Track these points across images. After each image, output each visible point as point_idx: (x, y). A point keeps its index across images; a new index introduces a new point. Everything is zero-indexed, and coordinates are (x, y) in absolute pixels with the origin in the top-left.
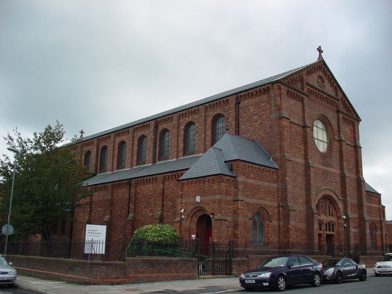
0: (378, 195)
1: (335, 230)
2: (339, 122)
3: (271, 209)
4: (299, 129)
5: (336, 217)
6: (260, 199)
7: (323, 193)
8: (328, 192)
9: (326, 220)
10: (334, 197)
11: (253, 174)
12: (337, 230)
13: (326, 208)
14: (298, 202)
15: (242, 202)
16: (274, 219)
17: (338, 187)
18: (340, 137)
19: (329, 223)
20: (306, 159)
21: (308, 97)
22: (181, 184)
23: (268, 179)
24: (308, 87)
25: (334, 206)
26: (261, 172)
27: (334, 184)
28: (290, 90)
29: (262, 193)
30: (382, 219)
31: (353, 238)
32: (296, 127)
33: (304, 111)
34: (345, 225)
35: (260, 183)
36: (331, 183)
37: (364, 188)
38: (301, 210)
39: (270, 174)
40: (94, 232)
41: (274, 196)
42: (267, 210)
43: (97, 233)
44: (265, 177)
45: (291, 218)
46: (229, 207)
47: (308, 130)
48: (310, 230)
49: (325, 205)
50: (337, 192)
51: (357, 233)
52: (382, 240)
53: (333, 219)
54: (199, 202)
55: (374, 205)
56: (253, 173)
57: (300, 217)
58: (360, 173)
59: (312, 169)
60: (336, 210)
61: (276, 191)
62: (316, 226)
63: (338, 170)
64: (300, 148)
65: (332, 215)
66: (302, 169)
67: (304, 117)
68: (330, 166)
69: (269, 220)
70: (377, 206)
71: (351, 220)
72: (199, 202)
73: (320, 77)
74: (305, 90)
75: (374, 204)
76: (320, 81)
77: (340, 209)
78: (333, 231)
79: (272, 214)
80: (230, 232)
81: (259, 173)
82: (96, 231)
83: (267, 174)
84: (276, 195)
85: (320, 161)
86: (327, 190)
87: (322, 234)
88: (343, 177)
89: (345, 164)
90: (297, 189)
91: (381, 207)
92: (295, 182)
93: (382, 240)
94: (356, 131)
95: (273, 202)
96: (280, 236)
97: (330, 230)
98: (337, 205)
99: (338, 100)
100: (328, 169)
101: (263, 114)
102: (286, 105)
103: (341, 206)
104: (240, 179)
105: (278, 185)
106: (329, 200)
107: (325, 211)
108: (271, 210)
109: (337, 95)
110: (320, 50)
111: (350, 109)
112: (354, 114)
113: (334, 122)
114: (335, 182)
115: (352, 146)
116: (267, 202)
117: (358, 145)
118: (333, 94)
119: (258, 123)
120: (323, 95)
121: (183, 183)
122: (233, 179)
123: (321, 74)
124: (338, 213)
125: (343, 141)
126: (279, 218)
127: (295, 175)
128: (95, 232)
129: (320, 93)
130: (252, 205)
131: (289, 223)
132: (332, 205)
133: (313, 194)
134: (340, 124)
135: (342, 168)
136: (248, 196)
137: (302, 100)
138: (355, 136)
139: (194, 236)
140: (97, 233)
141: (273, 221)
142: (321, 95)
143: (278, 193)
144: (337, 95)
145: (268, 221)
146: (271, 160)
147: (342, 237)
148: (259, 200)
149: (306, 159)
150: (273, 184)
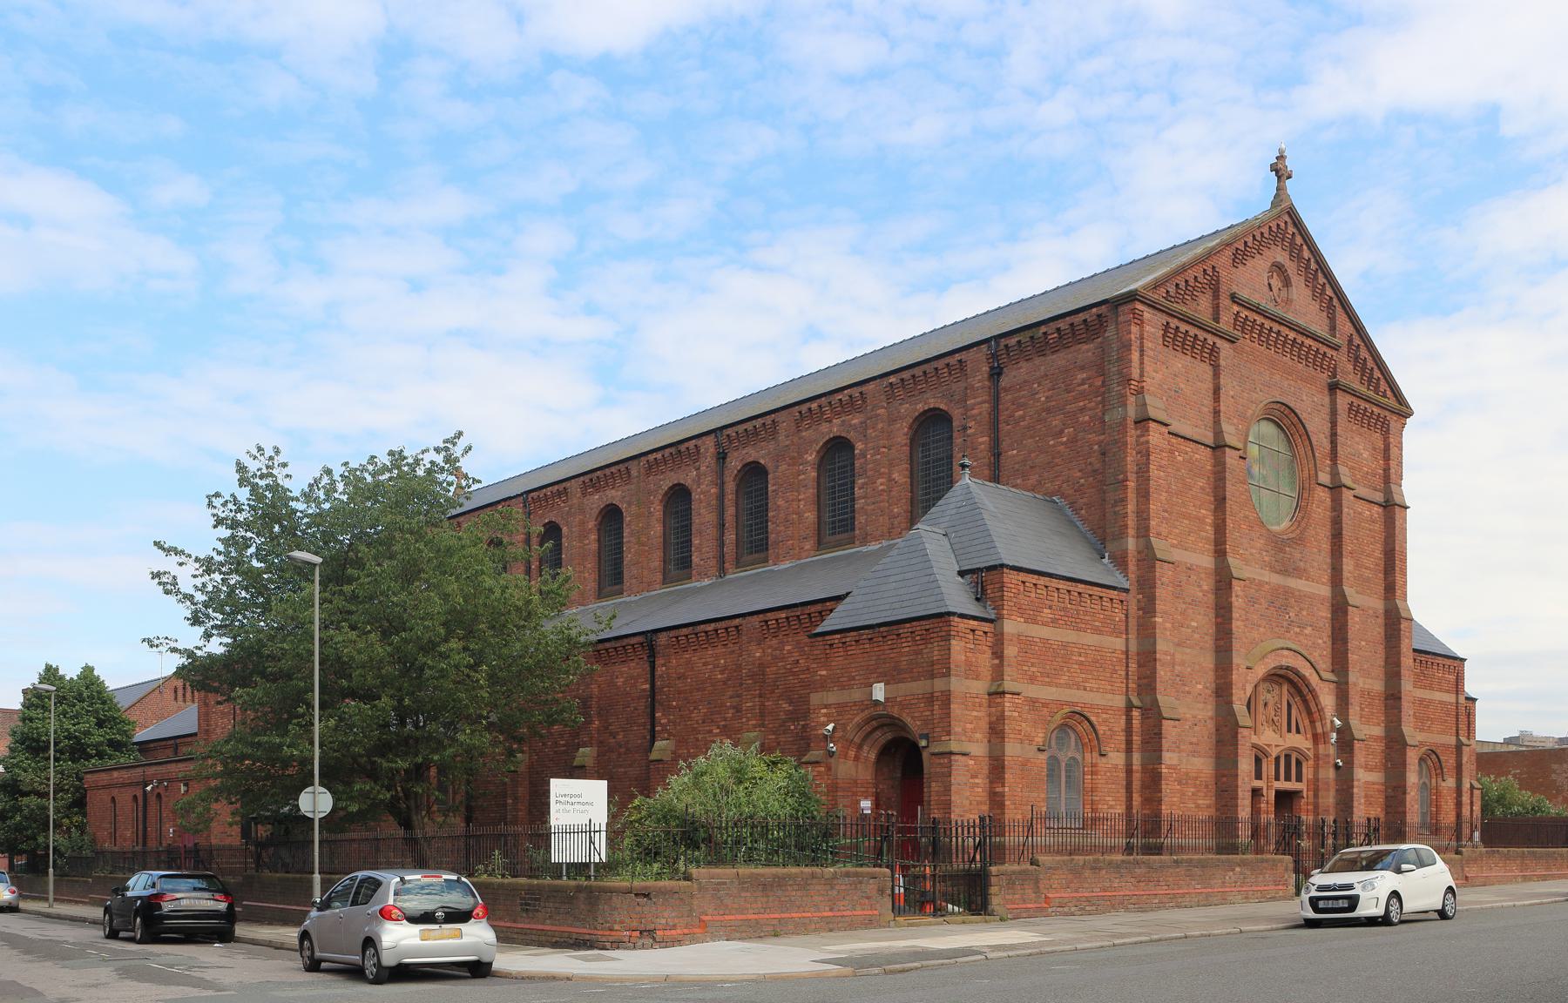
0: (1456, 663)
1: (1304, 779)
2: (1334, 424)
3: (1104, 716)
4: (1203, 456)
5: (1309, 736)
6: (1068, 686)
7: (1271, 663)
8: (1287, 657)
9: (1276, 746)
11: (1049, 611)
12: (1311, 777)
13: (1277, 710)
14: (1189, 693)
15: (1014, 696)
16: (1113, 746)
17: (1320, 641)
18: (1335, 474)
19: (1288, 757)
20: (1220, 552)
21: (1233, 342)
22: (822, 647)
23: (1097, 624)
24: (1236, 308)
25: (1305, 702)
26: (1074, 602)
27: (1308, 631)
28: (1174, 323)
29: (1077, 667)
30: (1463, 739)
31: (1363, 801)
33: (1216, 391)
34: (1339, 761)
35: (1070, 636)
37: (1407, 641)
38: (1200, 717)
39: (1102, 605)
40: (573, 800)
41: (1115, 675)
42: (1093, 719)
43: (583, 804)
44: (1087, 618)
45: (1165, 744)
46: (975, 713)
47: (1231, 457)
48: (1224, 779)
49: (1276, 698)
50: (1315, 656)
51: (1376, 786)
52: (1459, 804)
53: (1301, 742)
54: (883, 700)
55: (1438, 696)
56: (1050, 608)
57: (1194, 740)
58: (1398, 593)
59: (1237, 587)
60: (1310, 713)
61: (1120, 660)
62: (1245, 765)
63: (1323, 584)
64: (1201, 520)
65: (1298, 731)
66: (1205, 588)
67: (1217, 413)
68: (1298, 573)
69: (1097, 749)
70: (1450, 698)
71: (1357, 745)
72: (883, 700)
73: (1278, 268)
74: (1226, 323)
75: (1440, 690)
76: (1276, 283)
77: (1326, 710)
78: (1299, 779)
79: (1108, 733)
80: (980, 790)
81: (1069, 606)
82: (580, 796)
83: (1092, 606)
84: (1119, 672)
85: (1266, 559)
86: (1286, 652)
87: (1262, 789)
88: (1340, 608)
89: (1348, 565)
90: (1188, 651)
91: (1462, 699)
92: (1183, 629)
93: (1459, 804)
94: (1394, 451)
95: (1110, 696)
96: (1129, 799)
97: (1288, 778)
98: (1315, 697)
99: (1336, 348)
101: (1082, 410)
102: (1158, 376)
103: (1327, 700)
104: (1011, 626)
105: (1127, 639)
106: (1291, 682)
107: (1275, 719)
108: (1105, 721)
109: (1333, 329)
110: (1280, 171)
111: (1377, 374)
112: (1389, 393)
113: (1317, 425)
114: (1311, 626)
115: (1377, 504)
116: (1092, 694)
117: (1397, 499)
118: (1319, 326)
119: (1065, 439)
120: (1285, 331)
121: (829, 642)
122: (987, 627)
123: (1281, 256)
124: (1318, 724)
125: (1345, 486)
126: (1129, 742)
127: (1184, 606)
128: (578, 800)
129: (1276, 327)
130: (1045, 705)
131: (1159, 760)
132: (1298, 699)
133: (1238, 665)
134: (1339, 431)
135: (1336, 580)
136: (1032, 679)
137: (1214, 350)
138: (1387, 470)
139: (866, 805)
140: (583, 804)
141: (1110, 754)
142: (1278, 333)
143: (1127, 666)
144: (1333, 329)
145: (1095, 754)
146: (1106, 561)
147: (1329, 799)
148: (1068, 691)
149: (1220, 552)
150: (1113, 639)
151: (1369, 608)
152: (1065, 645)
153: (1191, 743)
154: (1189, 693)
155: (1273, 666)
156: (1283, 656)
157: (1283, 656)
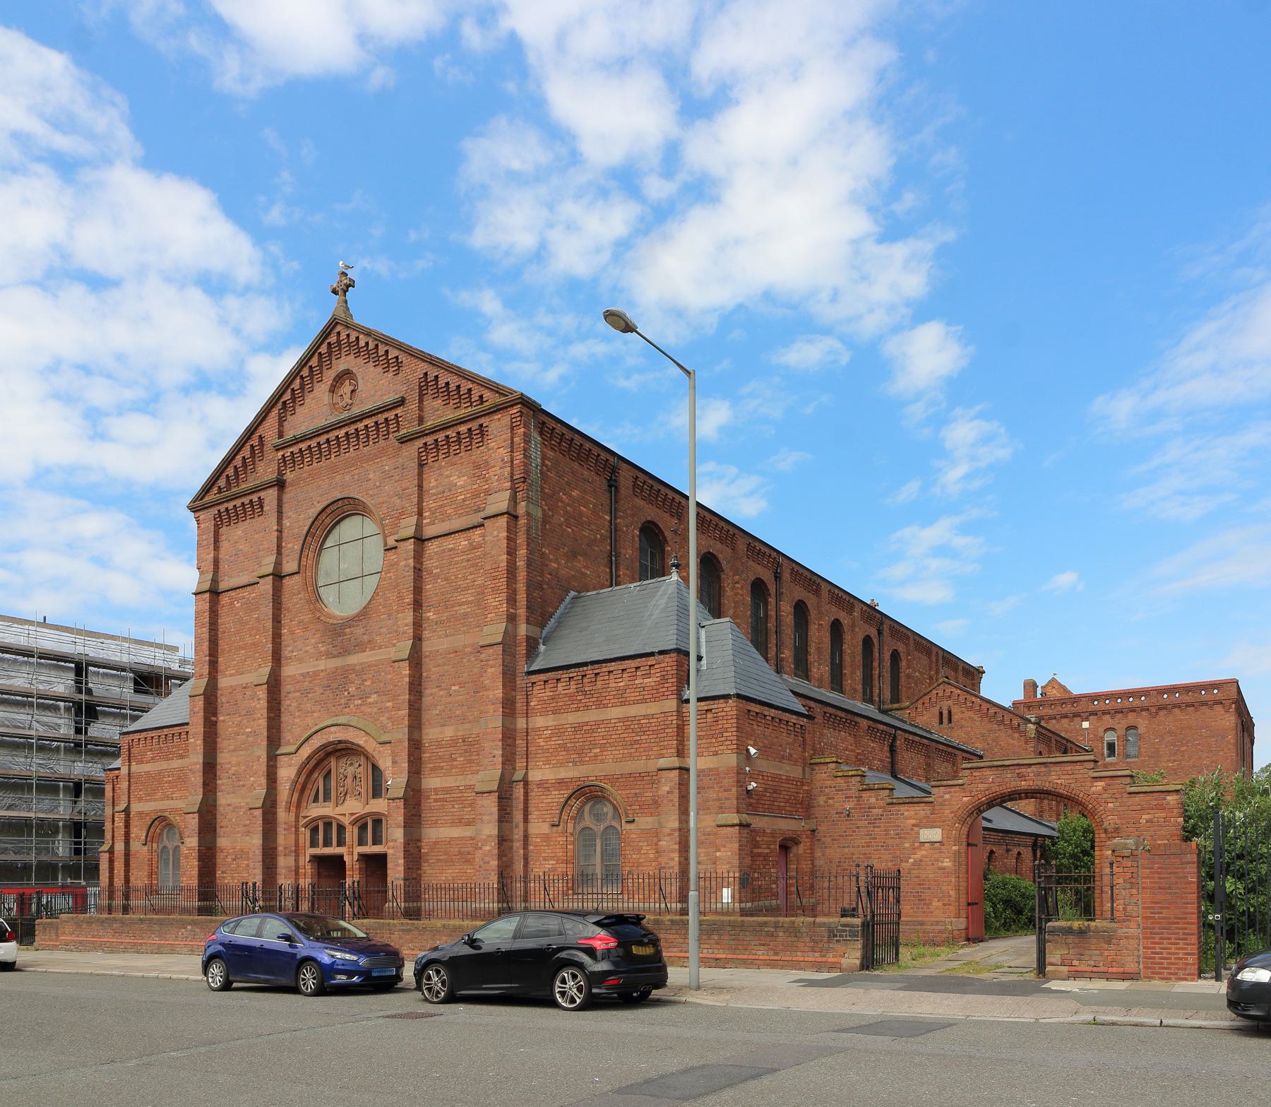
6: (162, 799)
9: (352, 814)
10: (361, 743)
14: (244, 786)
27: (374, 698)
32: (245, 593)
35: (163, 765)
56: (151, 750)
85: (322, 649)
90: (242, 753)
100: (352, 660)
116: (176, 801)
127: (239, 719)
151: (465, 646)
152: (160, 772)
153: (245, 826)
154: (244, 786)
155: (319, 744)
156: (331, 733)
157: (331, 733)
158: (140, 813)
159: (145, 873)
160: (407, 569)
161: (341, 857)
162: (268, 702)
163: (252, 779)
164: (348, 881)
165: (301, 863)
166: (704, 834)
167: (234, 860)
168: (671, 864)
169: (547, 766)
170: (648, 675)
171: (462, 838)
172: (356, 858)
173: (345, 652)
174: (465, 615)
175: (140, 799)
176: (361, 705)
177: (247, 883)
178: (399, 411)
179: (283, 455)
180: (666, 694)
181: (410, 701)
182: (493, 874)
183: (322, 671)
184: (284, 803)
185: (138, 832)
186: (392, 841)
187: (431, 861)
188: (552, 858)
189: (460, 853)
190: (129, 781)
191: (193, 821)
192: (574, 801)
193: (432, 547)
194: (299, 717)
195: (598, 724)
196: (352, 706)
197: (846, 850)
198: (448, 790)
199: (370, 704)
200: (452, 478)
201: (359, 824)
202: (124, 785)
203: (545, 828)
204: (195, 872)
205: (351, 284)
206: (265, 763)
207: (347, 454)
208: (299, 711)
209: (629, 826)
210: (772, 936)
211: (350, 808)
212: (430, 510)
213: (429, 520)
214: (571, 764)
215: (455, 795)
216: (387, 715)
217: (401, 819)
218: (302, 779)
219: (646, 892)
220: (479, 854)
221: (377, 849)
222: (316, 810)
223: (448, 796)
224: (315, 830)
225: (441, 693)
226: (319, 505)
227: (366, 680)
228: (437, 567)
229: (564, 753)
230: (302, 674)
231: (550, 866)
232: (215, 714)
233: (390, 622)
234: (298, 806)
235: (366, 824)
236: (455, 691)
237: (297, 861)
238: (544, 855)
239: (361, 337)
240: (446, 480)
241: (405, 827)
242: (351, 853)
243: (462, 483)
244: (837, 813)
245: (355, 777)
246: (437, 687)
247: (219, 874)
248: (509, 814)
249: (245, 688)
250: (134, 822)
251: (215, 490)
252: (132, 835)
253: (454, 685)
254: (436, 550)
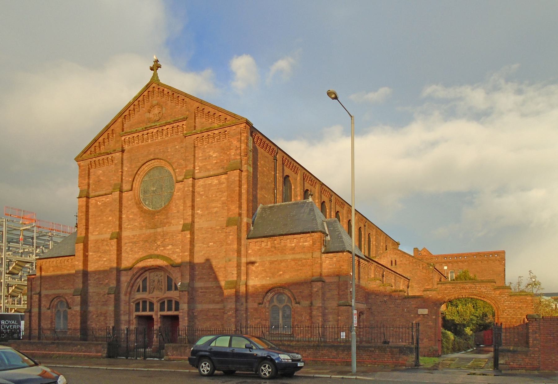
9: (157, 298)
14: (102, 284)
19: (170, 302)
27: (170, 247)
36: (163, 247)
97: (170, 309)
114: (171, 245)
116: (66, 290)
127: (100, 254)
153: (103, 301)
154: (102, 284)
158: (47, 296)
159: (49, 322)
160: (188, 191)
161: (152, 316)
162: (117, 247)
163: (107, 281)
164: (155, 327)
165: (131, 318)
166: (332, 309)
167: (97, 317)
168: (318, 321)
169: (256, 279)
170: (306, 241)
171: (215, 309)
172: (159, 317)
173: (155, 227)
174: (216, 212)
175: (46, 289)
176: (163, 250)
177: (109, 327)
178: (184, 123)
179: (125, 139)
180: (315, 249)
181: (190, 249)
182: (233, 324)
183: (143, 234)
184: (124, 292)
185: (45, 303)
186: (182, 309)
187: (199, 319)
188: (259, 318)
189: (213, 315)
190: (41, 280)
191: (78, 299)
192: (269, 294)
193: (200, 183)
194: (131, 254)
195: (281, 261)
196: (159, 250)
197: (384, 317)
198: (207, 288)
199: (168, 249)
200: (210, 153)
201: (160, 302)
202: (39, 282)
203: (255, 305)
204: (79, 322)
205: (159, 67)
206: (115, 274)
207: (157, 140)
208: (131, 251)
209: (296, 305)
210: (373, 352)
211: (155, 296)
212: (199, 166)
213: (198, 171)
214: (268, 278)
215: (211, 290)
216: (176, 255)
217: (186, 300)
218: (133, 281)
219: (305, 333)
220: (226, 316)
221: (176, 313)
222: (139, 296)
223: (208, 290)
224: (138, 304)
225: (204, 246)
226: (142, 161)
227: (166, 239)
228: (202, 191)
229: (265, 273)
230: (133, 235)
231: (258, 322)
232: (87, 252)
233: (178, 214)
234: (130, 293)
235: (164, 302)
236: (211, 245)
237: (129, 317)
238: (255, 317)
239: (166, 89)
240: (208, 154)
241: (188, 303)
242: (157, 315)
243: (215, 155)
244: (380, 302)
245: (159, 281)
246: (202, 243)
247: (89, 323)
248: (239, 299)
249: (103, 240)
250: (43, 299)
251: (89, 152)
252: (42, 305)
253: (211, 242)
254: (202, 184)
